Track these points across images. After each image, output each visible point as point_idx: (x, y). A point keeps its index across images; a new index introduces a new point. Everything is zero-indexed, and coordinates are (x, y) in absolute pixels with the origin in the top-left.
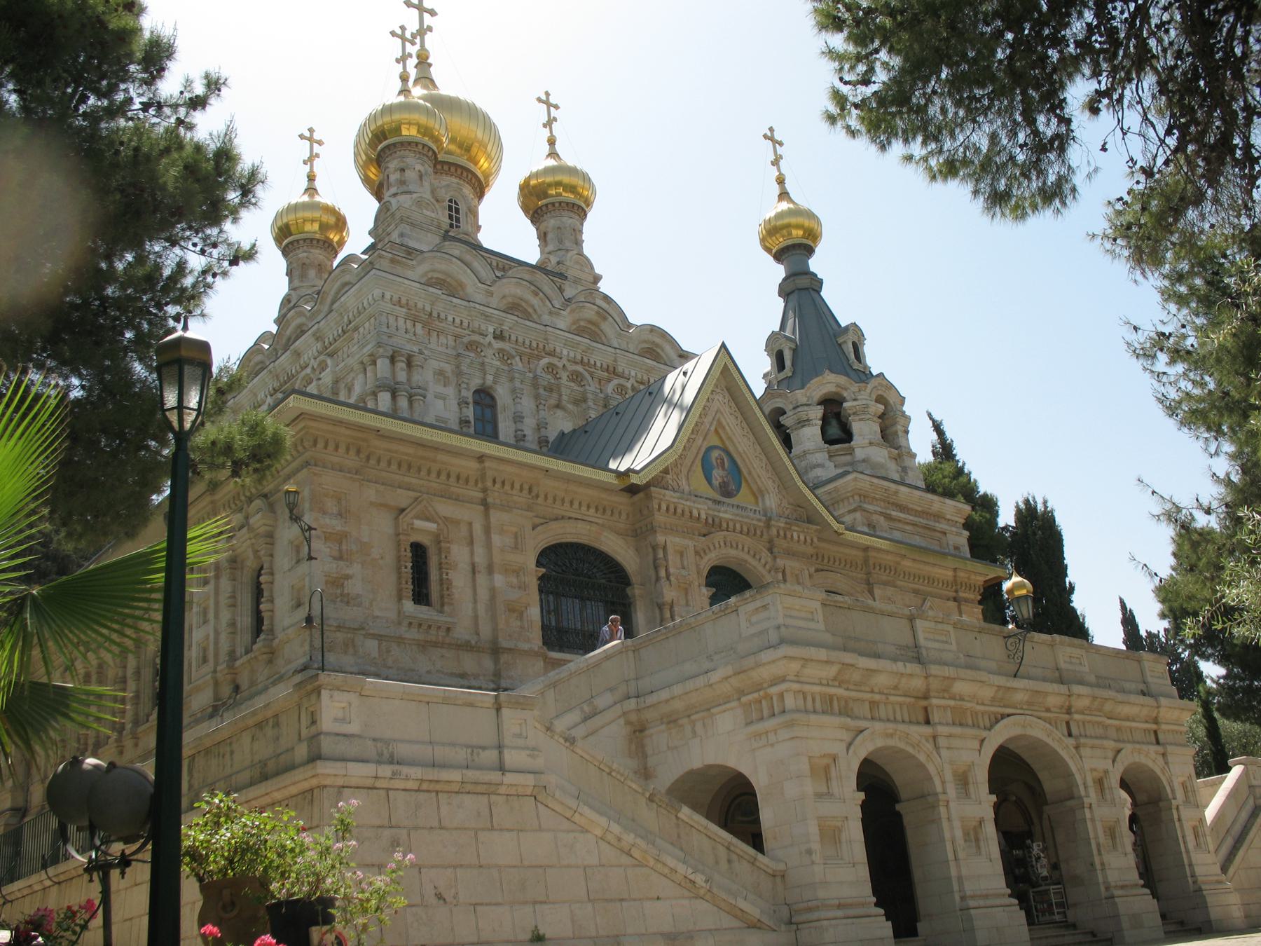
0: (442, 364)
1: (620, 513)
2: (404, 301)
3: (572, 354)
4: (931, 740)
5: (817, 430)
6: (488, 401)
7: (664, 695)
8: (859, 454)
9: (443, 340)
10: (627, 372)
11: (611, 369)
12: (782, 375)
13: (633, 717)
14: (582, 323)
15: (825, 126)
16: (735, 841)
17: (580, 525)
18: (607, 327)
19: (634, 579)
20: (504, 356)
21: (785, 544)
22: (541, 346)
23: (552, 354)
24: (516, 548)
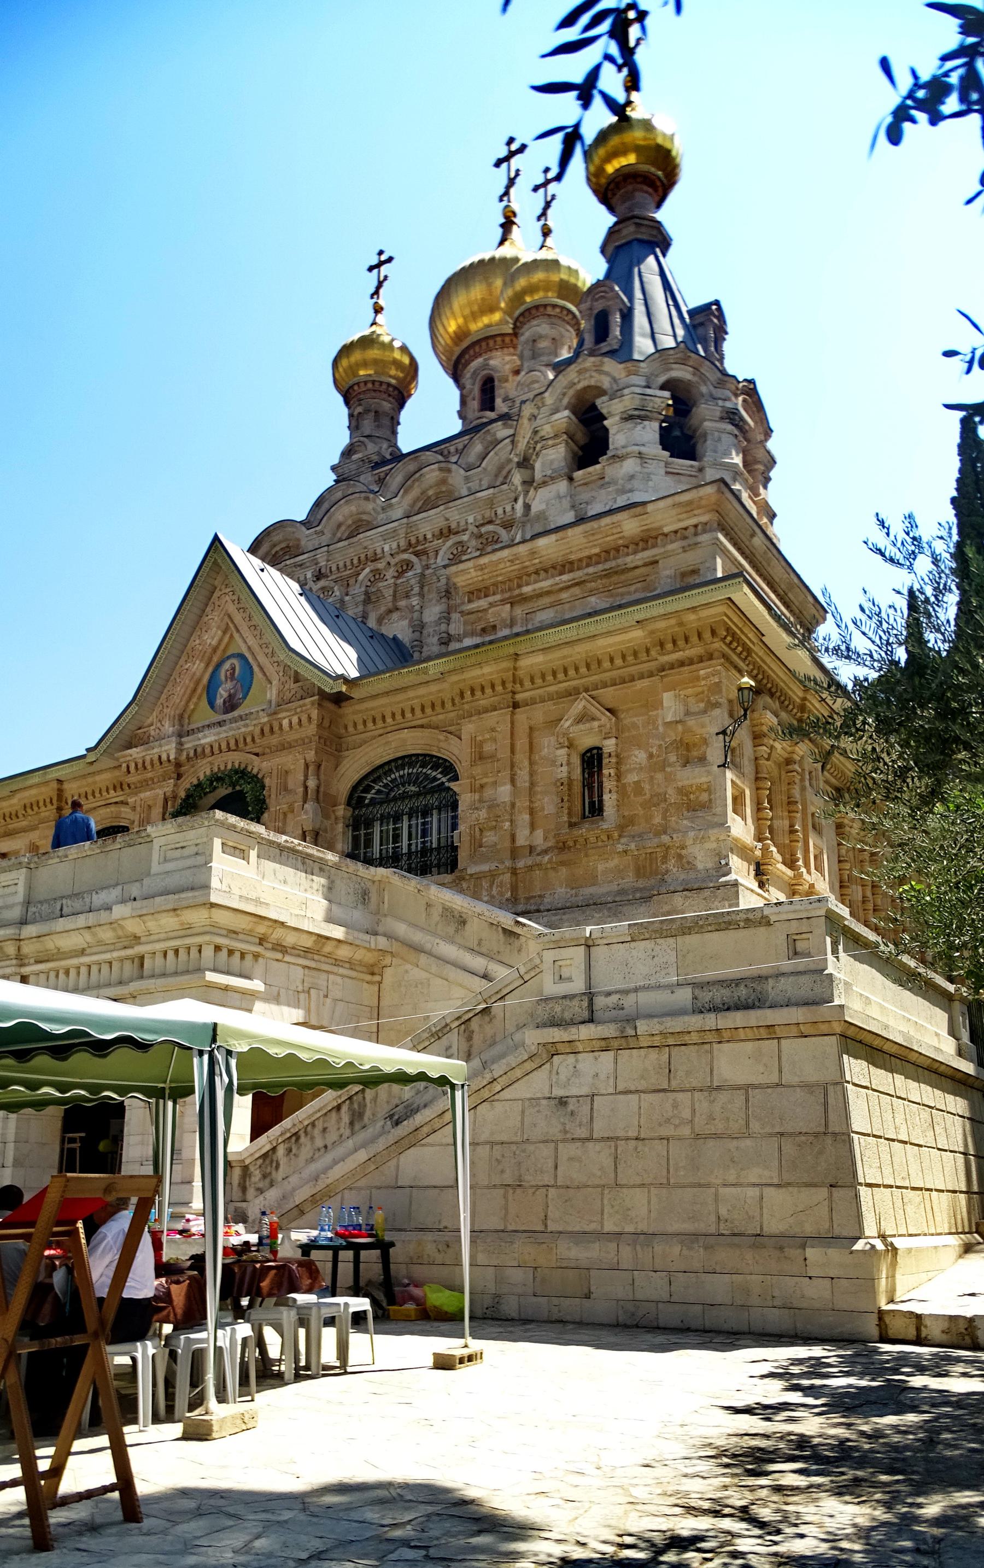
3: (394, 545)
11: (445, 531)
14: (430, 493)
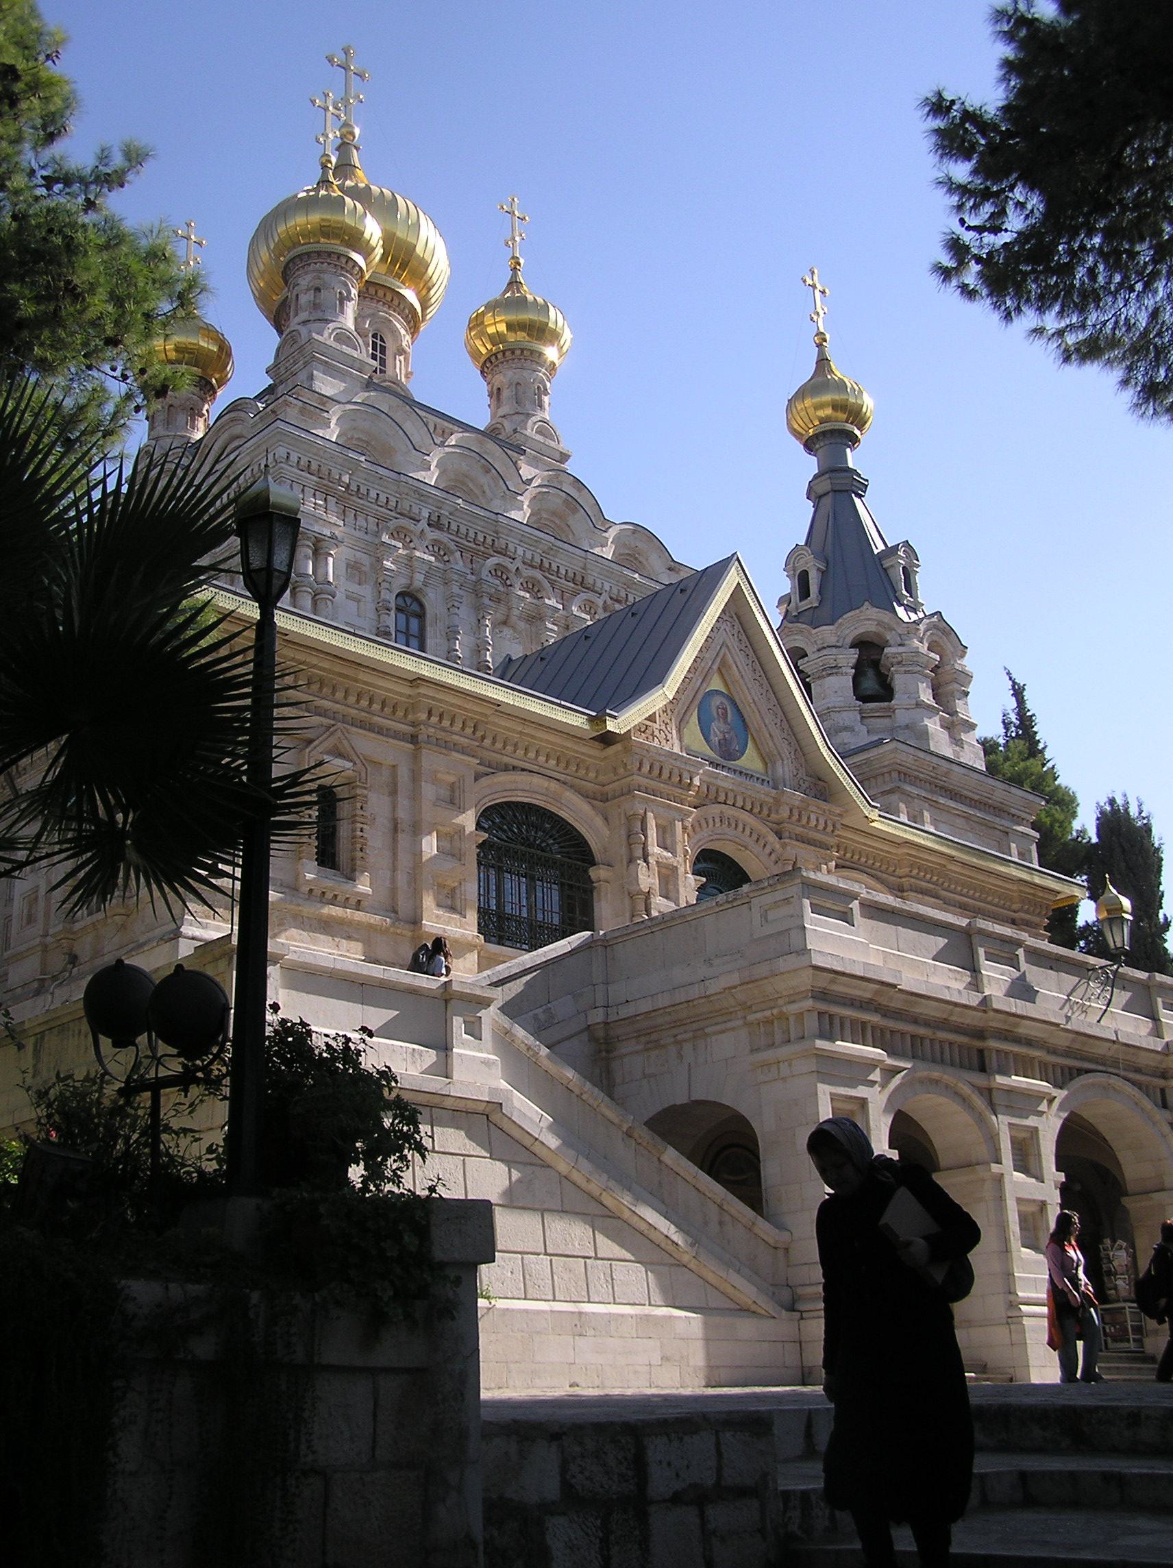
0: (359, 554)
1: (587, 769)
2: (314, 467)
3: (529, 556)
4: (986, 1093)
5: (848, 682)
6: (415, 607)
7: (644, 1006)
8: (902, 717)
9: (361, 521)
10: (599, 584)
11: (579, 578)
12: (805, 605)
13: (600, 1034)
15: (935, 280)
16: (730, 1196)
17: (536, 780)
18: (578, 523)
19: (598, 857)
20: (438, 549)
21: (799, 830)
22: (489, 540)
23: (503, 553)
24: (452, 802)
